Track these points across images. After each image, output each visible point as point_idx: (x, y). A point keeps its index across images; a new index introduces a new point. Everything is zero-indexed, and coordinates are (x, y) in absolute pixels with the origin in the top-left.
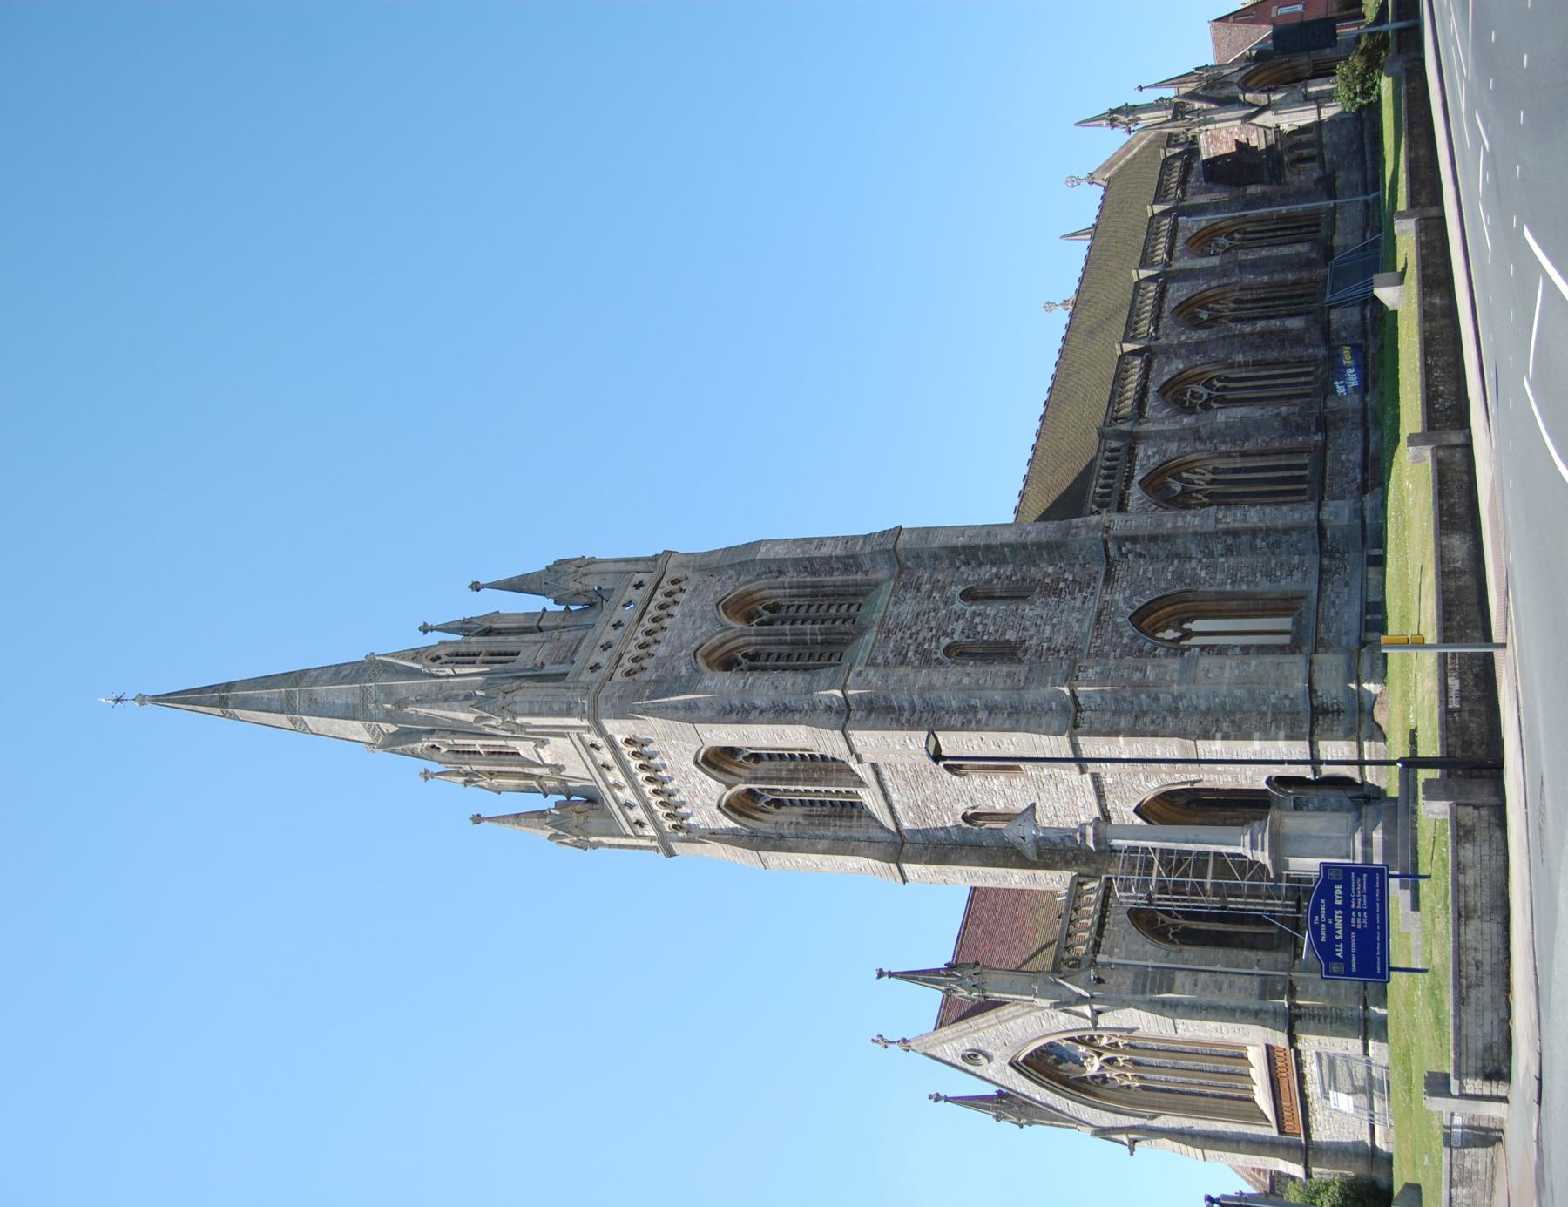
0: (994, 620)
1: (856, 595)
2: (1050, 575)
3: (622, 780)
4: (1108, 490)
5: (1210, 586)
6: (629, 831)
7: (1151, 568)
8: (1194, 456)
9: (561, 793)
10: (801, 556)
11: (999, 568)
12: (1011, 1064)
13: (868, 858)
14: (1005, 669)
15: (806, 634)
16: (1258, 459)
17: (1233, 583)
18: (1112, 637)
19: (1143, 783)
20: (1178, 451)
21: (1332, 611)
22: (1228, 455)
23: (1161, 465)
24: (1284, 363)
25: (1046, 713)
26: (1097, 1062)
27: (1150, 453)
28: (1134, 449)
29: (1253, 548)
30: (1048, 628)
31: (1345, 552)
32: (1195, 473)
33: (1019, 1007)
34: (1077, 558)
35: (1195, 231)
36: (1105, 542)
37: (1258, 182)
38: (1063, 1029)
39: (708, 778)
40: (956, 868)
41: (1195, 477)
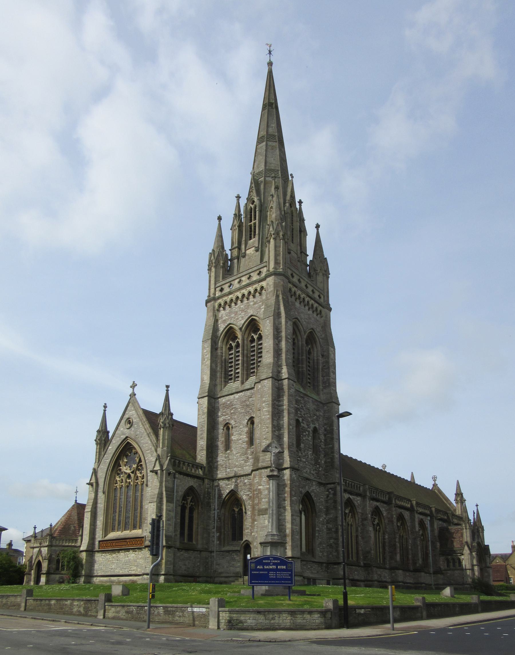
0: (308, 438)
1: (314, 385)
2: (321, 462)
3: (244, 283)
4: (347, 486)
5: (318, 522)
6: (218, 285)
7: (323, 500)
8: (357, 518)
9: (231, 256)
10: (330, 364)
11: (324, 443)
12: (127, 437)
13: (209, 384)
14: (295, 443)
15: (302, 364)
16: (355, 541)
17: (318, 531)
18: (302, 484)
19: (245, 494)
20: (359, 512)
21: (309, 566)
22: (357, 531)
23: (355, 506)
24: (384, 553)
25: (278, 458)
26: (128, 471)
27: (358, 502)
28: (360, 496)
29: (330, 538)
30: (304, 460)
31: (328, 572)
32: (351, 518)
33: (155, 442)
34: (327, 473)
35: (425, 522)
36: (334, 483)
37: (441, 546)
38: (146, 459)
39: (245, 320)
40: (206, 419)
41: (350, 518)
